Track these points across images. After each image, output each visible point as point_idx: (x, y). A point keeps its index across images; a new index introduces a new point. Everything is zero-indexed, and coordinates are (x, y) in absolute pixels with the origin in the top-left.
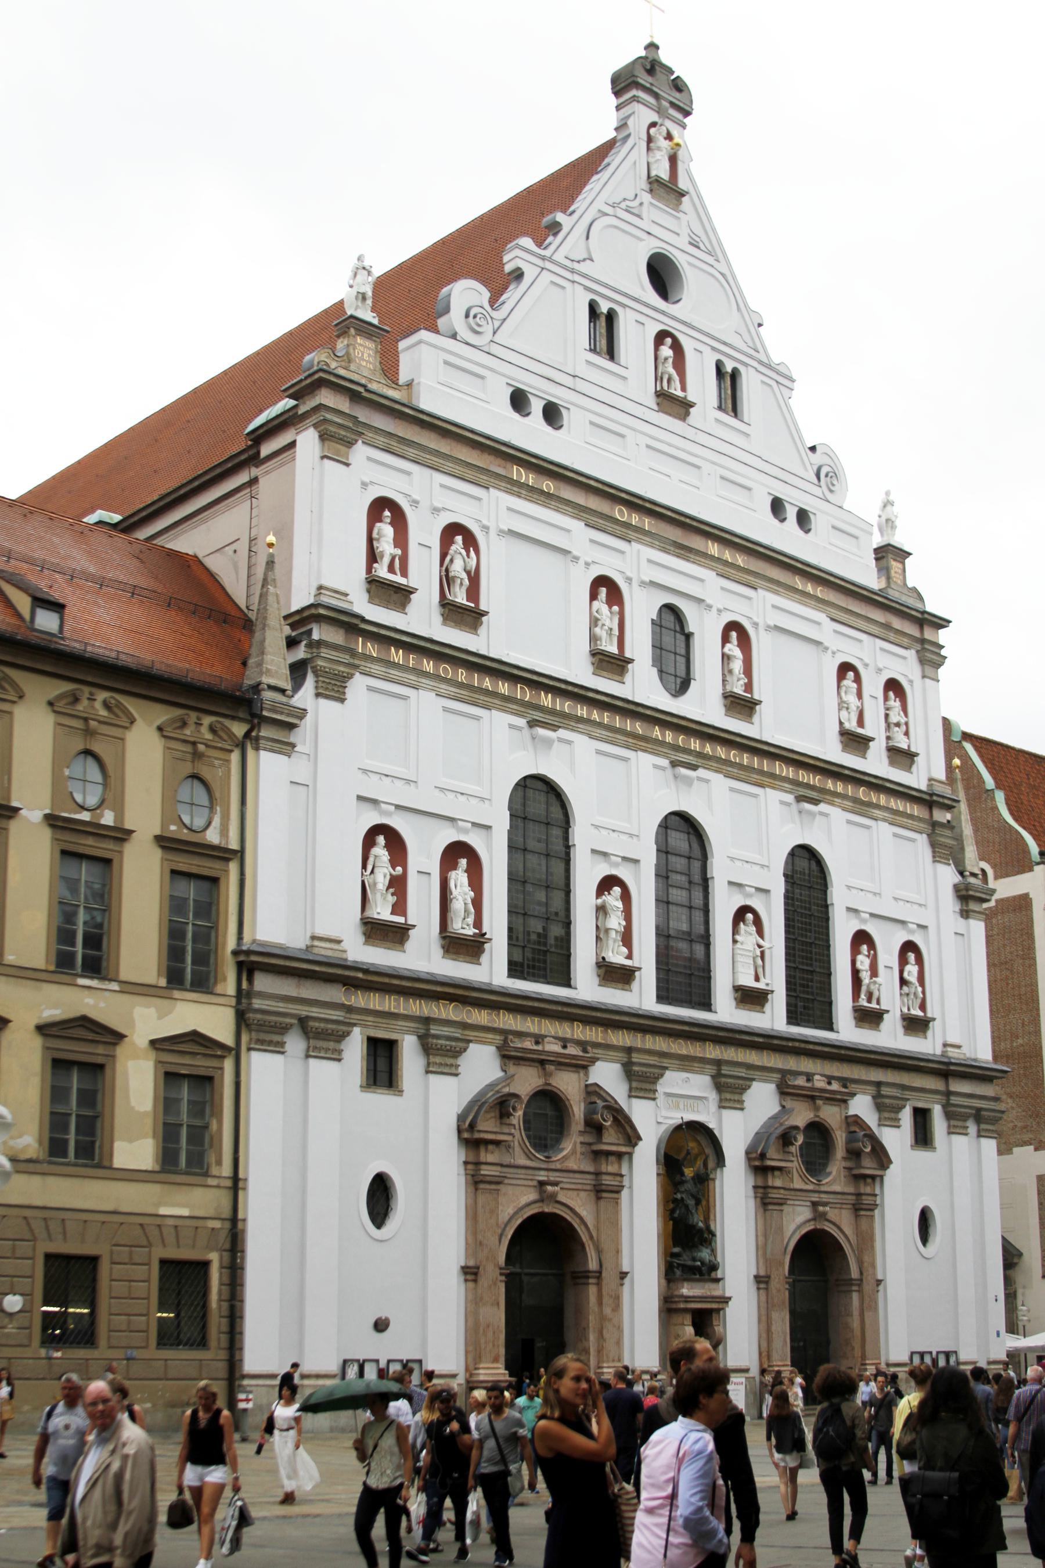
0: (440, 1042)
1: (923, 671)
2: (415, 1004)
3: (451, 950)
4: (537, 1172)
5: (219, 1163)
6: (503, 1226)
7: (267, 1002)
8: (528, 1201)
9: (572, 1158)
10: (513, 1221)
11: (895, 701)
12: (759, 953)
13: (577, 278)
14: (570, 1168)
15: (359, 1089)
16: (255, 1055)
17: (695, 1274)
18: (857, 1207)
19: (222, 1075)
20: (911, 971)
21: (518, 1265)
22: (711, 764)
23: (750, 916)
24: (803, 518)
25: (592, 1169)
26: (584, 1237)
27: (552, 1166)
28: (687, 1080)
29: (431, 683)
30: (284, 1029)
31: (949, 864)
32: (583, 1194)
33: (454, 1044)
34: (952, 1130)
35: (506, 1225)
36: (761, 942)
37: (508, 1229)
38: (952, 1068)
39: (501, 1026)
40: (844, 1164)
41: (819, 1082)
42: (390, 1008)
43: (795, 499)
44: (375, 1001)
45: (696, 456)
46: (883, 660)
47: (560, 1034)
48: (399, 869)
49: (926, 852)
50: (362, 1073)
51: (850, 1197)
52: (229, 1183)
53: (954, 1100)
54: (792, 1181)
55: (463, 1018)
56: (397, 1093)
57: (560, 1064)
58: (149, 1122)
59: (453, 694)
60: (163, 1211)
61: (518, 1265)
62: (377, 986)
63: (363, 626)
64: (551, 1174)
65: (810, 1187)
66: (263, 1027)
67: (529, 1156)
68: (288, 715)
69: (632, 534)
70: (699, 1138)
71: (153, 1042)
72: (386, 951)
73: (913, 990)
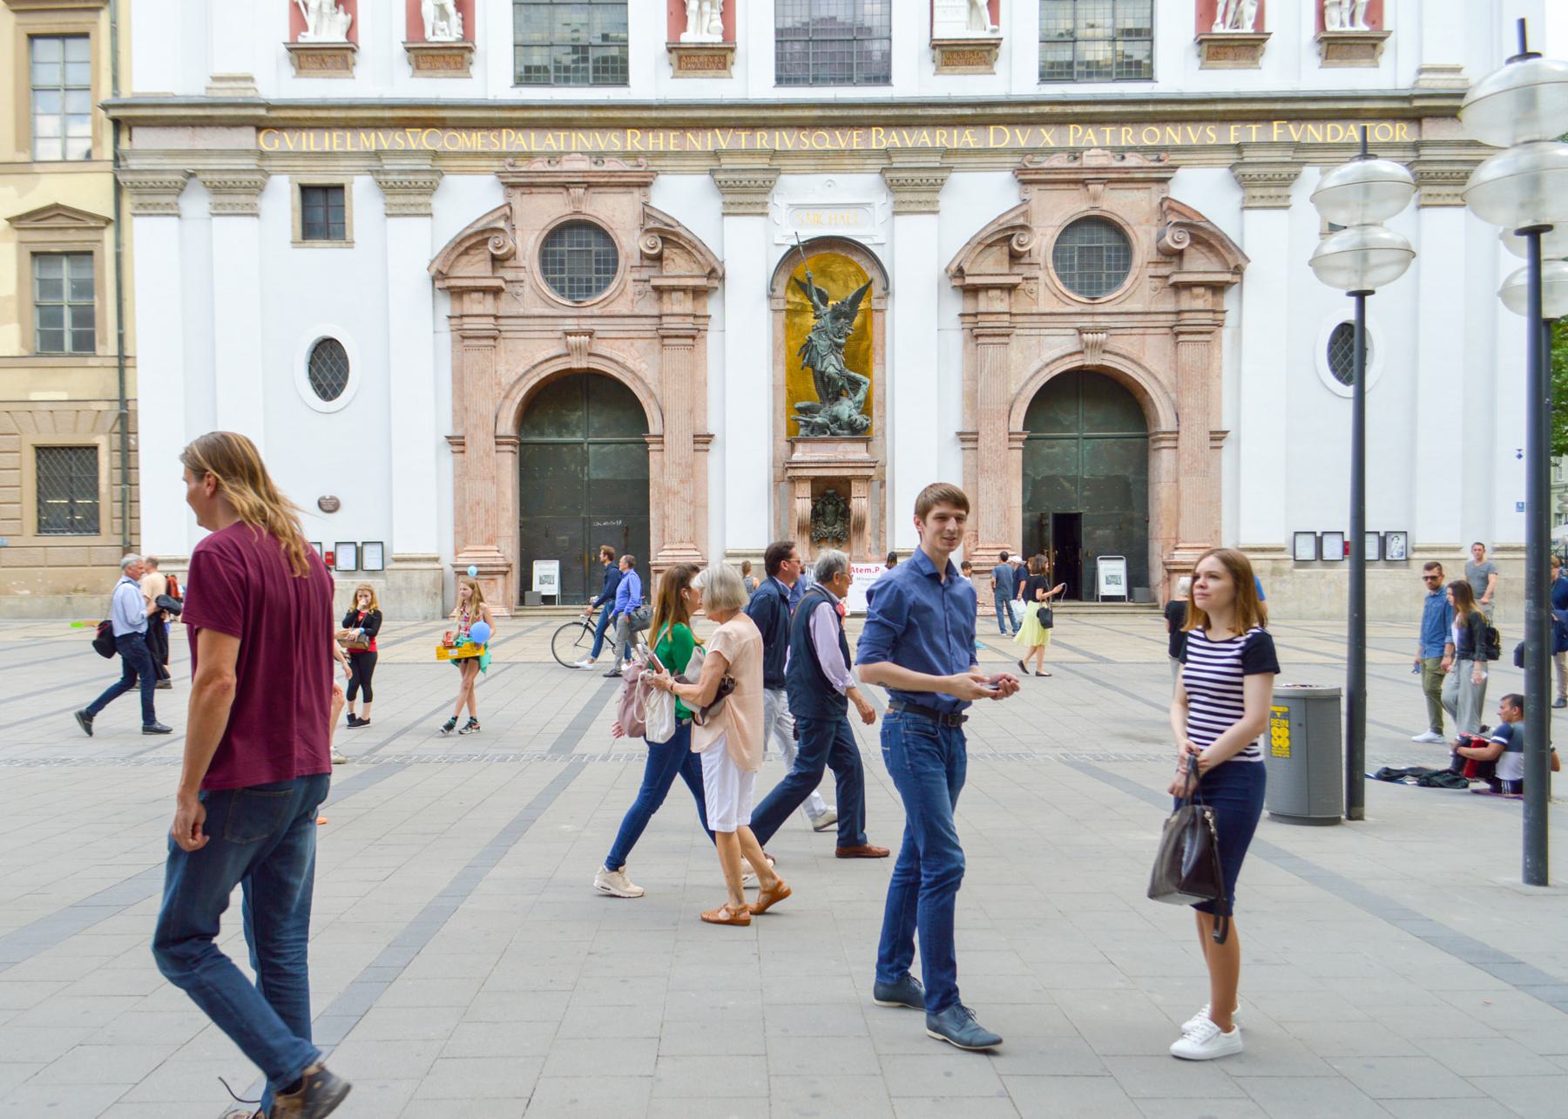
0: (389, 177)
2: (368, 138)
3: (422, 65)
4: (560, 321)
5: (104, 342)
6: (508, 388)
7: (148, 161)
8: (548, 356)
9: (621, 300)
10: (524, 381)
14: (616, 313)
15: (290, 245)
16: (138, 221)
17: (825, 433)
18: (1177, 329)
19: (102, 248)
21: (579, 434)
25: (655, 312)
26: (641, 396)
27: (587, 312)
28: (830, 184)
30: (179, 189)
32: (639, 343)
33: (411, 177)
34: (1423, 202)
35: (513, 387)
37: (515, 391)
38: (1418, 103)
39: (504, 148)
40: (1152, 271)
41: (1092, 159)
42: (308, 146)
44: (308, 141)
47: (589, 147)
50: (293, 227)
51: (1162, 317)
52: (115, 362)
53: (1427, 153)
54: (1036, 301)
55: (443, 146)
56: (344, 245)
57: (589, 185)
58: (12, 306)
60: (34, 396)
61: (579, 434)
62: (309, 124)
64: (582, 321)
65: (1077, 308)
66: (138, 189)
67: (547, 302)
70: (854, 259)
71: (10, 220)
72: (327, 80)
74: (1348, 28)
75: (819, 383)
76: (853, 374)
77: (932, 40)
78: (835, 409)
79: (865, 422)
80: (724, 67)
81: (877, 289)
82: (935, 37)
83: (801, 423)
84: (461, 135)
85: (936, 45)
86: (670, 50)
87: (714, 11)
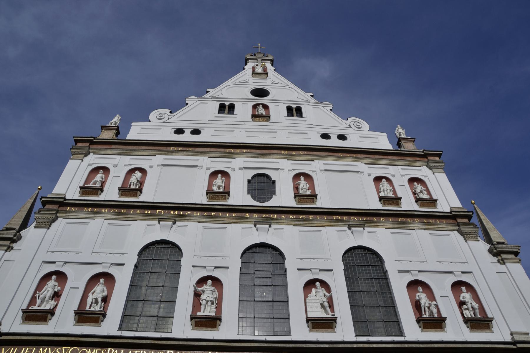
1: (433, 171)
11: (418, 185)
12: (325, 299)
13: (212, 99)
20: (466, 296)
22: (283, 222)
23: (318, 284)
24: (342, 137)
29: (102, 216)
31: (479, 241)
36: (328, 295)
43: (334, 133)
45: (275, 129)
46: (403, 172)
48: (59, 288)
49: (461, 238)
59: (115, 218)
63: (67, 202)
68: (7, 234)
69: (234, 155)
73: (470, 305)
74: (474, 317)
77: (307, 318)
80: (215, 326)
82: (308, 316)
84: (88, 351)
85: (308, 320)
86: (192, 319)
87: (212, 305)
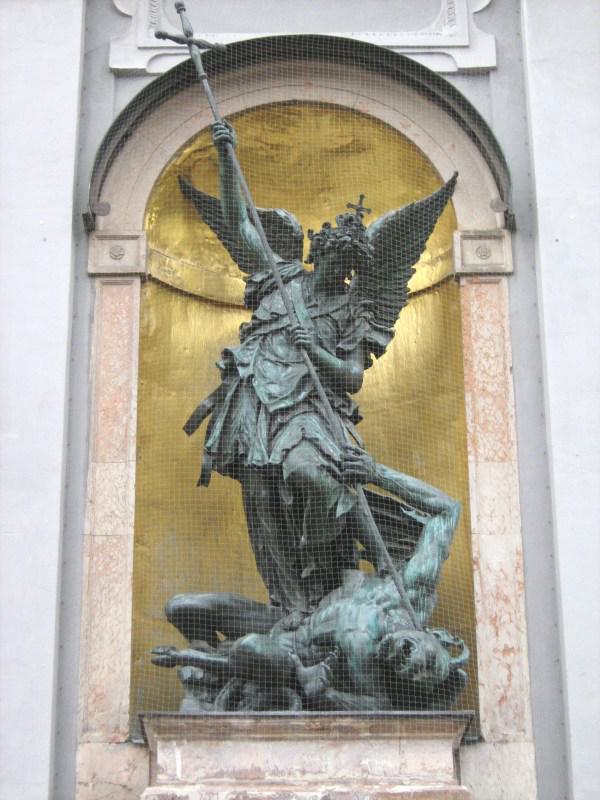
75: (267, 525)
76: (391, 474)
78: (327, 610)
79: (445, 661)
81: (472, 210)
83: (187, 672)
